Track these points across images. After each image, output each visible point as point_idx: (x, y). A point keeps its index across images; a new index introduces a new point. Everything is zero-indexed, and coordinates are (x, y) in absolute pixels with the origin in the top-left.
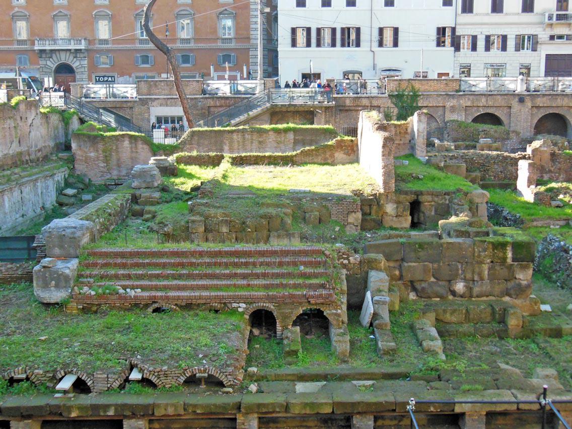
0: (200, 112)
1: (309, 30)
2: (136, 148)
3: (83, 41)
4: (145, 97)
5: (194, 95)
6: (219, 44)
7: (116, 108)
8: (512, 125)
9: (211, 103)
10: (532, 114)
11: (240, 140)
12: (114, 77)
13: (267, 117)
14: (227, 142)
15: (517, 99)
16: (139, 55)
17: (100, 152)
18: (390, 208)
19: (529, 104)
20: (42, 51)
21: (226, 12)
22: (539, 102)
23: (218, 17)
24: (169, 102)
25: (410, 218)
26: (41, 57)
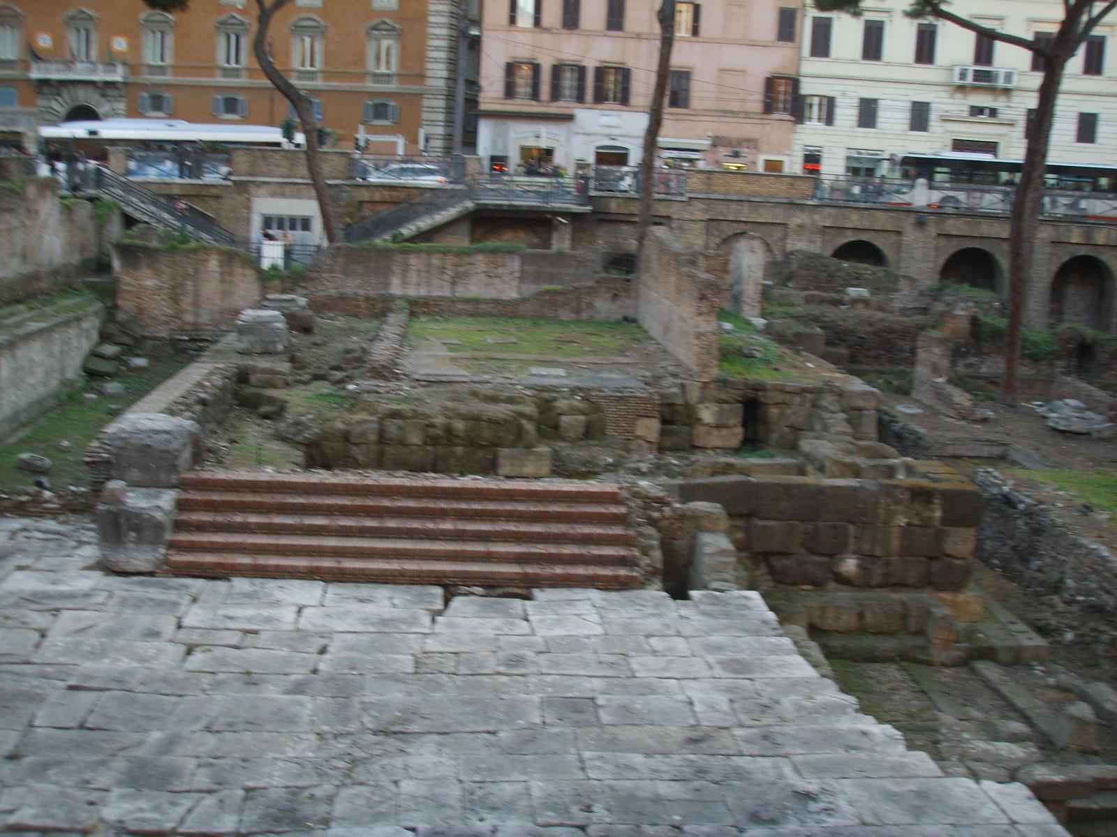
1: (536, 68)
2: (231, 274)
8: (903, 264)
9: (365, 195)
10: (937, 249)
13: (465, 228)
15: (912, 219)
16: (219, 97)
17: (165, 278)
18: (707, 414)
19: (932, 230)
20: (45, 83)
21: (385, 27)
22: (952, 226)
24: (287, 189)
25: (739, 431)
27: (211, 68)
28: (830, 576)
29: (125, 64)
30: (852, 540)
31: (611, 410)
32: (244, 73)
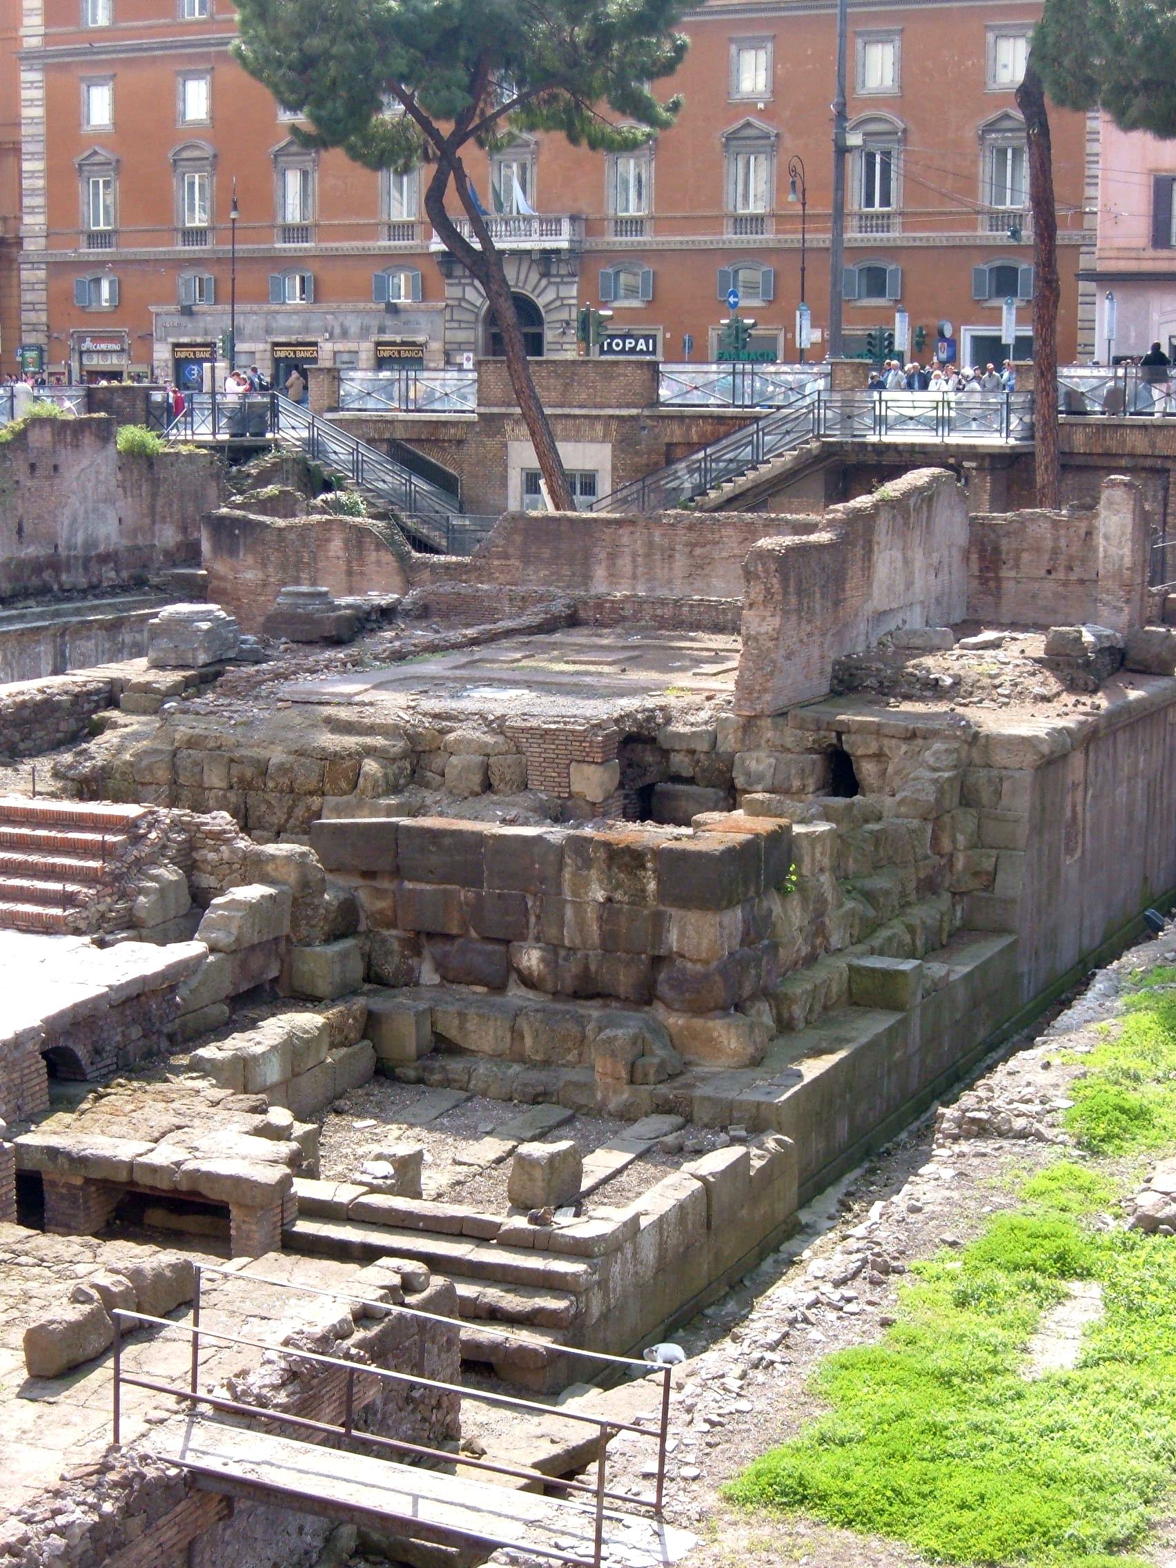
0: (644, 460)
2: (361, 559)
3: (566, 226)
4: (495, 410)
5: (628, 406)
6: (980, 233)
7: (419, 441)
11: (640, 548)
12: (654, 337)
13: (817, 485)
14: (603, 555)
21: (1007, 124)
23: (982, 138)
26: (449, 275)
27: (716, 218)
28: (514, 976)
29: (573, 219)
30: (533, 919)
31: (534, 751)
32: (770, 225)
